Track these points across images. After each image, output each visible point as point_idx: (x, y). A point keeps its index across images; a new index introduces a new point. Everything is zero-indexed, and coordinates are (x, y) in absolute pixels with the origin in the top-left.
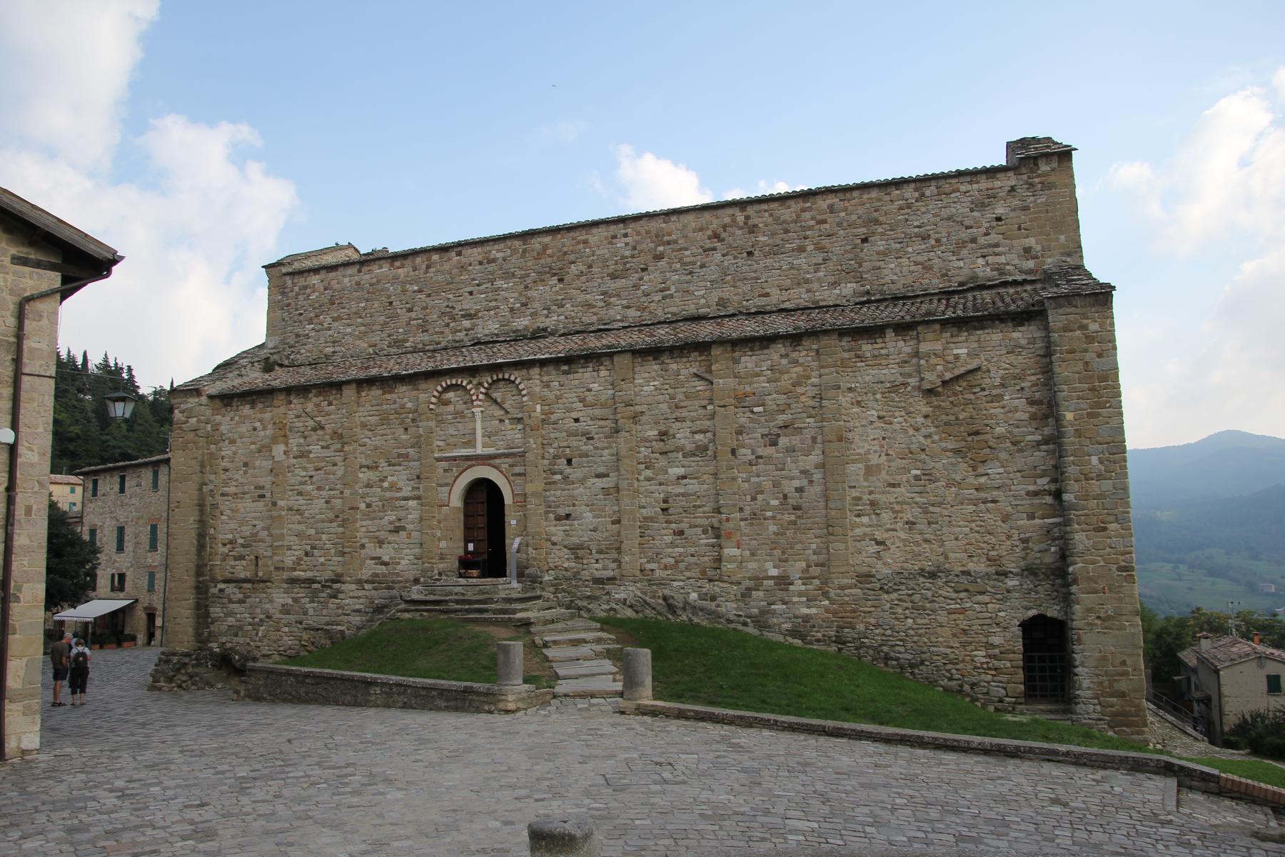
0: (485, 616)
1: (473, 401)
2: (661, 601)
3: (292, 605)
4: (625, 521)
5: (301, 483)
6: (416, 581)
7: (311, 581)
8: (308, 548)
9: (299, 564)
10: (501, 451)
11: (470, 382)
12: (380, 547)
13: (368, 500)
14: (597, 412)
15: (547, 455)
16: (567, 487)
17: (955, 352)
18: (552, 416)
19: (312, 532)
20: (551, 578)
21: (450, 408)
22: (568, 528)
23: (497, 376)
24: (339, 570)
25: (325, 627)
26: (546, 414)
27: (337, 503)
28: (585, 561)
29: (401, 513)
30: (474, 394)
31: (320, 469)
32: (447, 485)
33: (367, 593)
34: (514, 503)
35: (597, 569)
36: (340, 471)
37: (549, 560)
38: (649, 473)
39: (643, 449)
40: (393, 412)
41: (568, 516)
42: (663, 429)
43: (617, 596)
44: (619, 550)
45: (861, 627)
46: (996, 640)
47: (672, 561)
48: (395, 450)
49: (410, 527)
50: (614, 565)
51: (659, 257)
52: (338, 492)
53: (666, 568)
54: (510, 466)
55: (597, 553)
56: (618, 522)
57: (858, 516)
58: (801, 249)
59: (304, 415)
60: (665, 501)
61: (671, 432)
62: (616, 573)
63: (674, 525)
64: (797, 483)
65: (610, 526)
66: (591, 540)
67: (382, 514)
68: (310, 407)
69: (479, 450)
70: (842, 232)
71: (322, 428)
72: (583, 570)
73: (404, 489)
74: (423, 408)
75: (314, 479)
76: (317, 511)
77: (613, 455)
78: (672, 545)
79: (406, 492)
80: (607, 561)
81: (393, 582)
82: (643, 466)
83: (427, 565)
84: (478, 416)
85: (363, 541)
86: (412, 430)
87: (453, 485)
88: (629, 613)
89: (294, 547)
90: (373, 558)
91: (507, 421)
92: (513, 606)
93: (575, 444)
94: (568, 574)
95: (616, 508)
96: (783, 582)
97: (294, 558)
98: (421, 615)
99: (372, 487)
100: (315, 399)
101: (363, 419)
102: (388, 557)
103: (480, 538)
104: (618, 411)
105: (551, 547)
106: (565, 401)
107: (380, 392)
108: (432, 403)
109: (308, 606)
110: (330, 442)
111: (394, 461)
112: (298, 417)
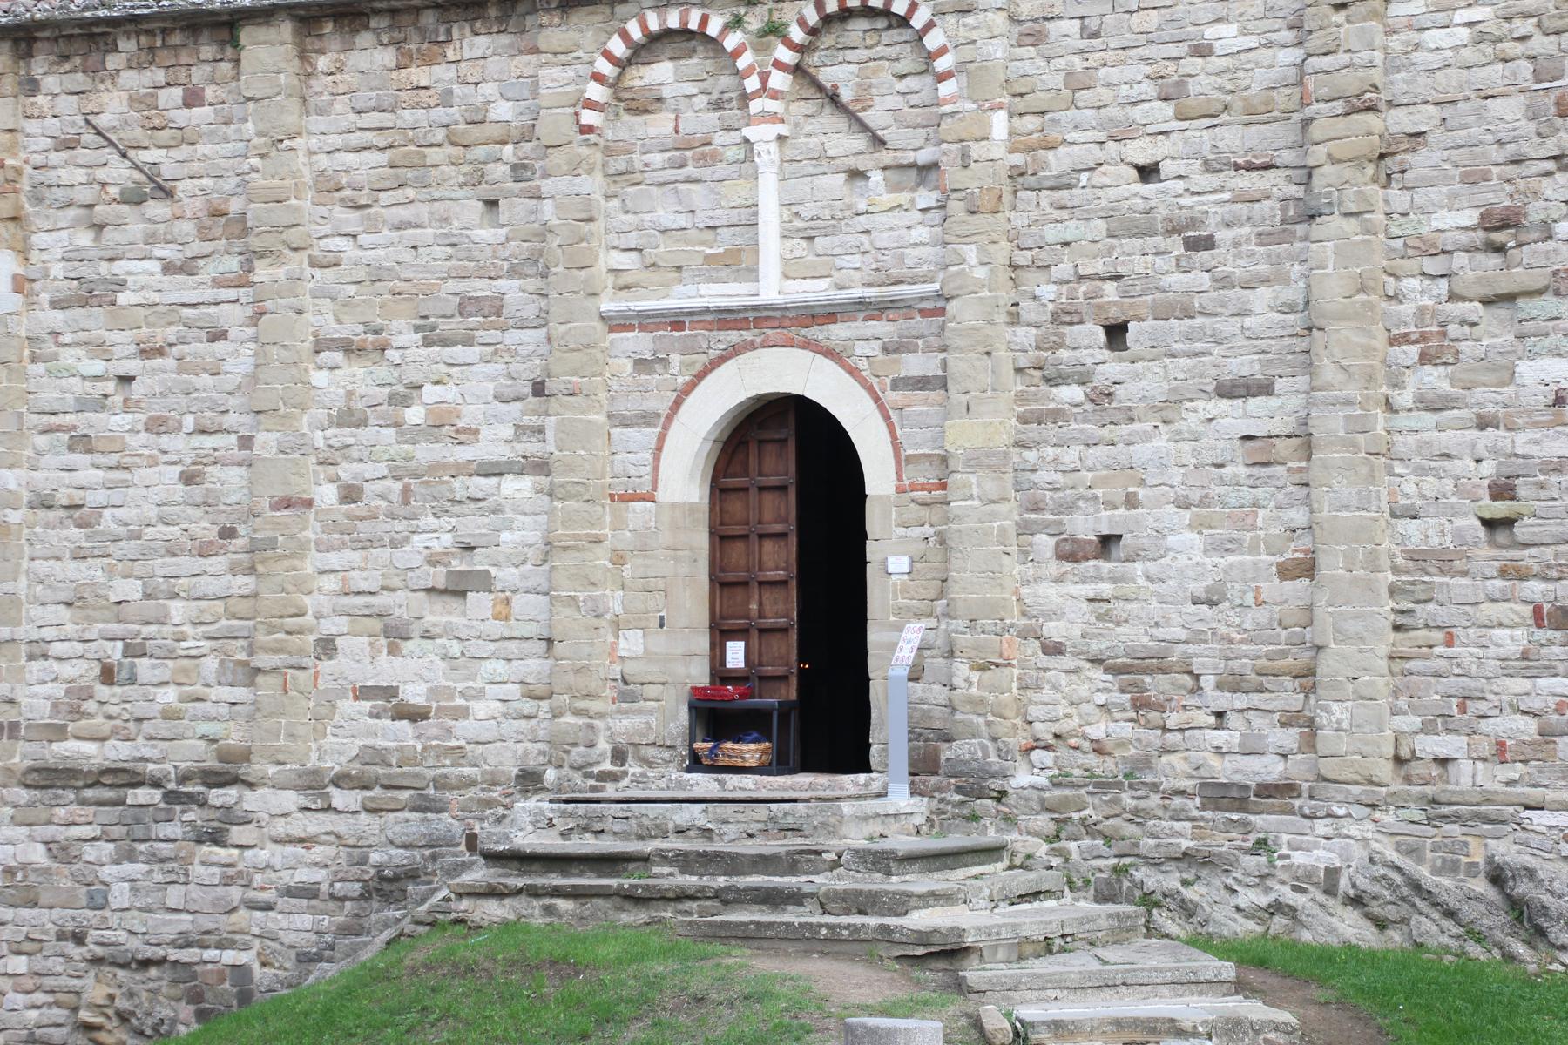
0: (791, 916)
1: (745, 98)
2: (1480, 886)
3: (46, 872)
4: (1332, 565)
5: (84, 405)
6: (529, 780)
7: (125, 776)
8: (115, 651)
9: (77, 713)
10: (857, 292)
11: (737, 22)
12: (393, 651)
13: (346, 471)
14: (1233, 138)
15: (1028, 310)
16: (1106, 433)
18: (1050, 155)
19: (130, 589)
20: (1042, 780)
21: (660, 125)
22: (1106, 589)
24: (235, 736)
25: (174, 954)
26: (1029, 150)
27: (229, 481)
28: (1173, 720)
29: (473, 525)
30: (750, 71)
31: (160, 352)
32: (646, 419)
33: (341, 825)
34: (900, 490)
35: (1218, 751)
36: (238, 359)
37: (1034, 711)
38: (1435, 379)
39: (1415, 283)
40: (440, 135)
41: (1107, 542)
42: (1501, 199)
43: (1299, 858)
44: (1307, 677)
47: (1529, 727)
48: (451, 285)
49: (506, 575)
50: (1289, 738)
52: (233, 439)
53: (1501, 752)
55: (1220, 686)
56: (1307, 568)
59: (89, 137)
60: (1501, 491)
61: (1535, 211)
62: (1297, 769)
63: (1535, 589)
65: (1273, 587)
66: (1196, 637)
67: (400, 526)
68: (112, 107)
69: (771, 288)
71: (166, 192)
72: (1165, 751)
73: (485, 433)
74: (556, 124)
75: (137, 389)
76: (152, 513)
77: (1289, 308)
78: (1528, 663)
79: (494, 444)
80: (1258, 721)
81: (441, 783)
82: (1413, 351)
83: (569, 719)
84: (768, 156)
85: (331, 626)
86: (514, 209)
87: (669, 419)
88: (1350, 927)
89: (57, 649)
90: (363, 693)
91: (876, 177)
92: (896, 883)
93: (1140, 264)
94: (1107, 767)
95: (1298, 516)
97: (58, 690)
98: (549, 910)
99: (363, 422)
100: (130, 78)
101: (323, 161)
102: (422, 688)
103: (769, 622)
104: (1316, 132)
105: (1044, 660)
106: (1105, 94)
107: (388, 56)
108: (590, 105)
109: (108, 872)
110: (197, 247)
111: (445, 326)
112: (68, 144)
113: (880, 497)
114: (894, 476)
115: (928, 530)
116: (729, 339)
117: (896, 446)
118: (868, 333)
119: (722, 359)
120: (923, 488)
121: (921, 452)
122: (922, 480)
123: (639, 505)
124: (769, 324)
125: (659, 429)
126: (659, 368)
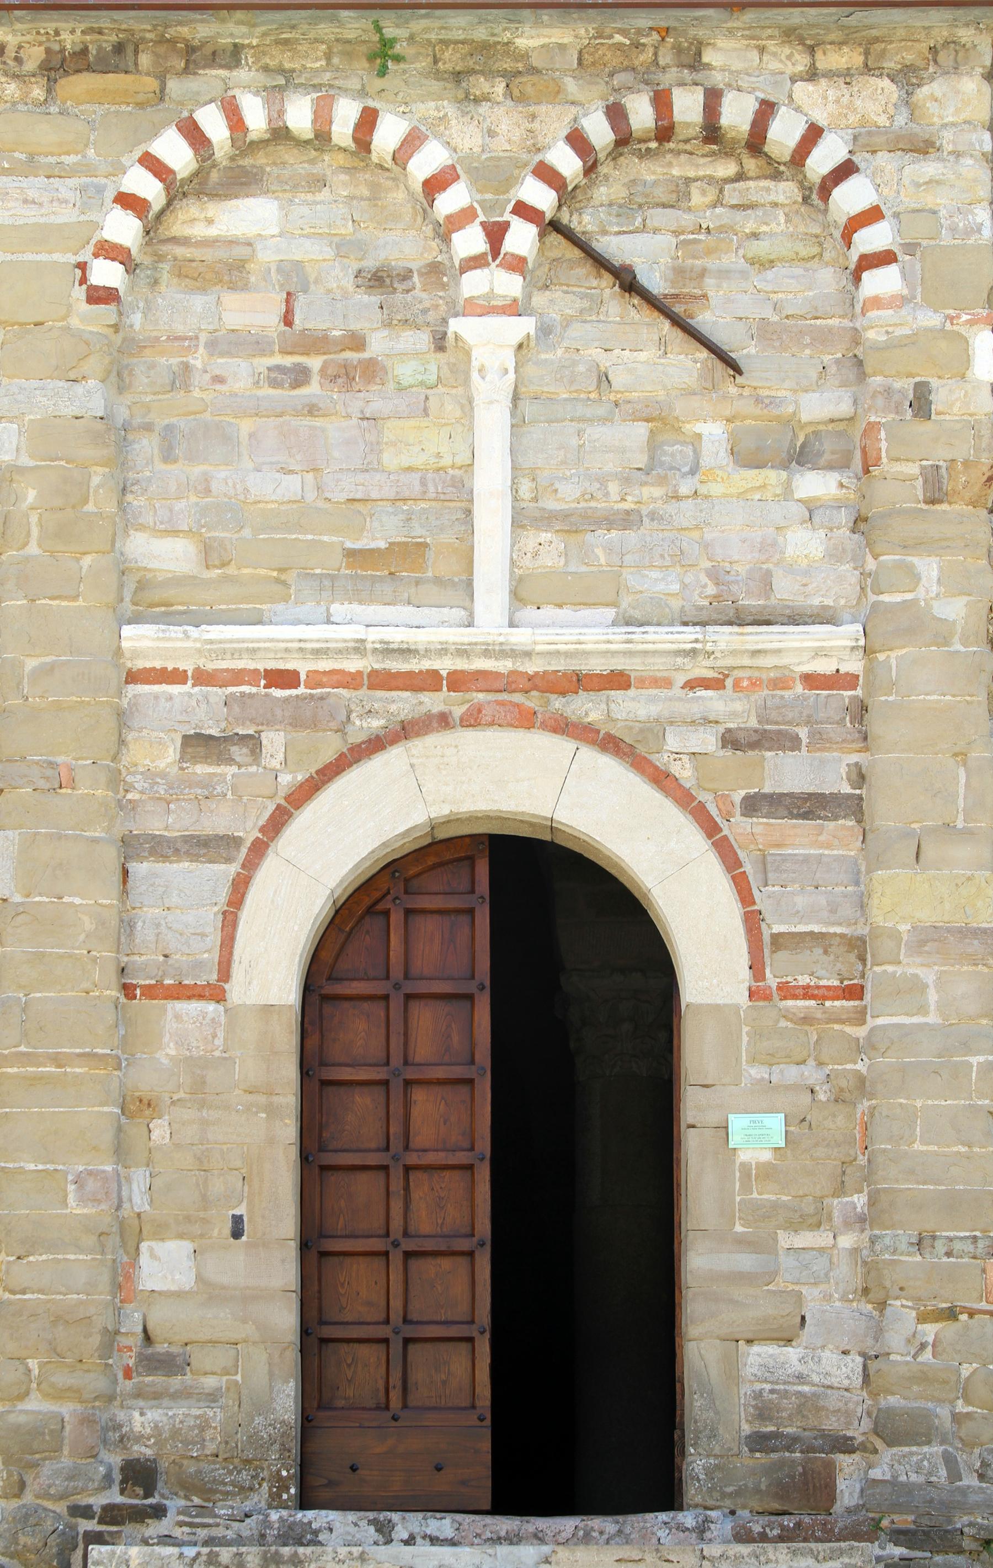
23: (662, 102)
54: (730, 741)
87: (259, 850)
108: (109, 251)
113: (716, 1009)
114: (746, 974)
115: (811, 1074)
116: (393, 708)
117: (753, 921)
118: (696, 710)
119: (376, 745)
120: (806, 993)
121: (802, 928)
122: (804, 980)
123: (194, 1007)
124: (481, 684)
125: (233, 869)
126: (237, 752)
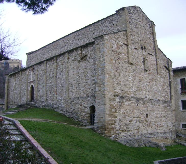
17: (84, 52)
45: (69, 109)
46: (86, 111)
51: (67, 43)
57: (70, 87)
58: (85, 37)
64: (63, 82)
70: (91, 33)
78: (50, 95)
96: (61, 100)
